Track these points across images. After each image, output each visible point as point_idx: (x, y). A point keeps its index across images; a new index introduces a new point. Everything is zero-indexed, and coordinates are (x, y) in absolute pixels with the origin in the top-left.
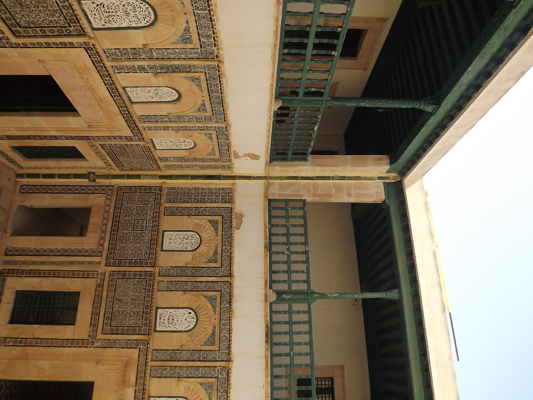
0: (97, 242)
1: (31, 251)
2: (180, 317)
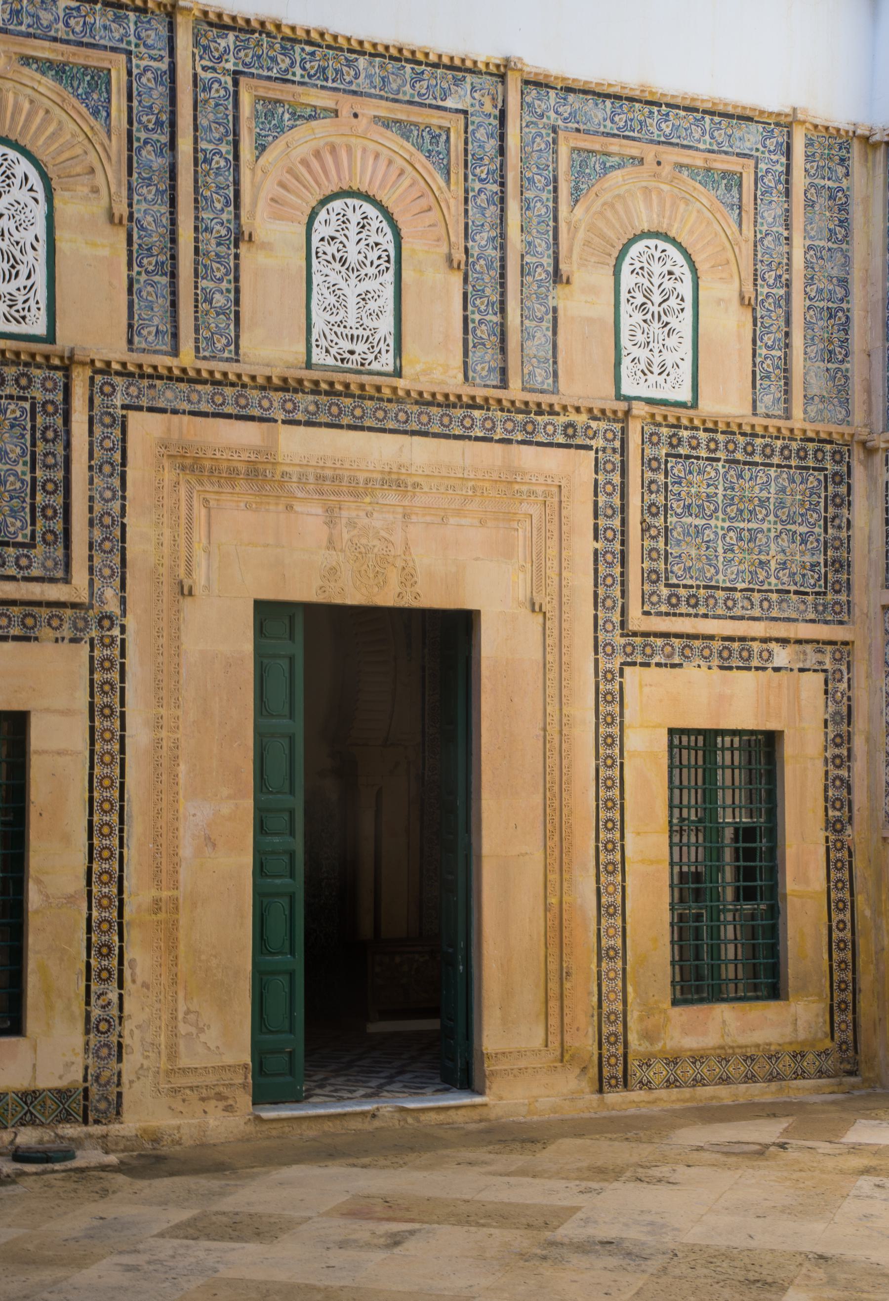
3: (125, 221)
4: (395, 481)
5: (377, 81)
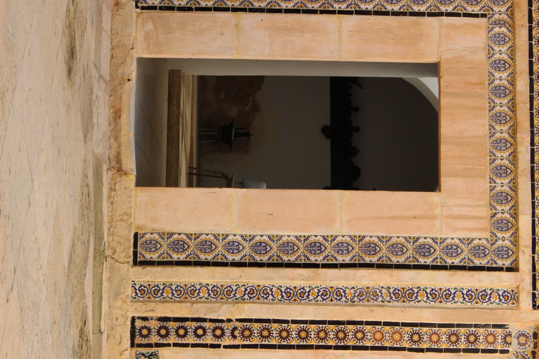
0: (486, 212)
1: (234, 247)
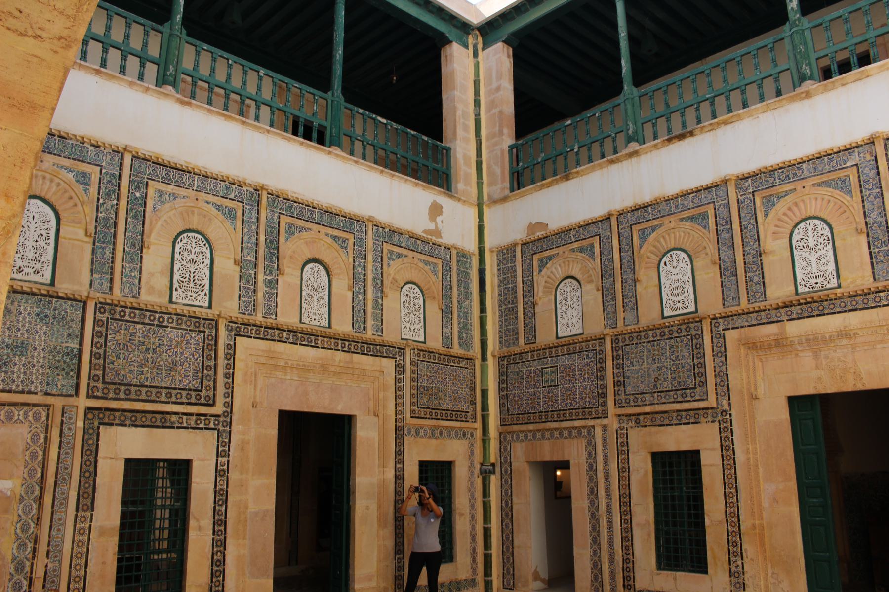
0: (575, 440)
1: (595, 553)
2: (673, 277)
3: (717, 261)
4: (845, 334)
5: (812, 170)
